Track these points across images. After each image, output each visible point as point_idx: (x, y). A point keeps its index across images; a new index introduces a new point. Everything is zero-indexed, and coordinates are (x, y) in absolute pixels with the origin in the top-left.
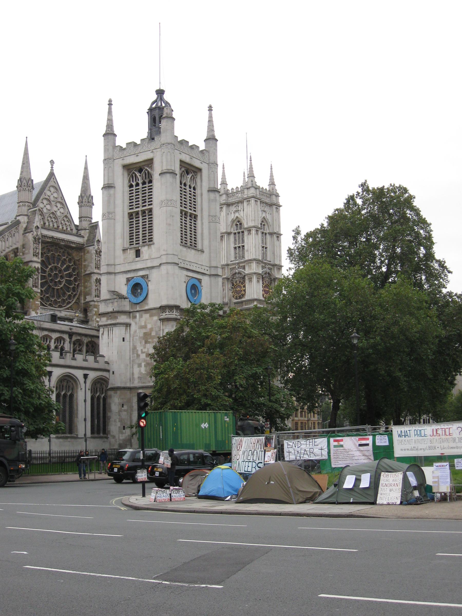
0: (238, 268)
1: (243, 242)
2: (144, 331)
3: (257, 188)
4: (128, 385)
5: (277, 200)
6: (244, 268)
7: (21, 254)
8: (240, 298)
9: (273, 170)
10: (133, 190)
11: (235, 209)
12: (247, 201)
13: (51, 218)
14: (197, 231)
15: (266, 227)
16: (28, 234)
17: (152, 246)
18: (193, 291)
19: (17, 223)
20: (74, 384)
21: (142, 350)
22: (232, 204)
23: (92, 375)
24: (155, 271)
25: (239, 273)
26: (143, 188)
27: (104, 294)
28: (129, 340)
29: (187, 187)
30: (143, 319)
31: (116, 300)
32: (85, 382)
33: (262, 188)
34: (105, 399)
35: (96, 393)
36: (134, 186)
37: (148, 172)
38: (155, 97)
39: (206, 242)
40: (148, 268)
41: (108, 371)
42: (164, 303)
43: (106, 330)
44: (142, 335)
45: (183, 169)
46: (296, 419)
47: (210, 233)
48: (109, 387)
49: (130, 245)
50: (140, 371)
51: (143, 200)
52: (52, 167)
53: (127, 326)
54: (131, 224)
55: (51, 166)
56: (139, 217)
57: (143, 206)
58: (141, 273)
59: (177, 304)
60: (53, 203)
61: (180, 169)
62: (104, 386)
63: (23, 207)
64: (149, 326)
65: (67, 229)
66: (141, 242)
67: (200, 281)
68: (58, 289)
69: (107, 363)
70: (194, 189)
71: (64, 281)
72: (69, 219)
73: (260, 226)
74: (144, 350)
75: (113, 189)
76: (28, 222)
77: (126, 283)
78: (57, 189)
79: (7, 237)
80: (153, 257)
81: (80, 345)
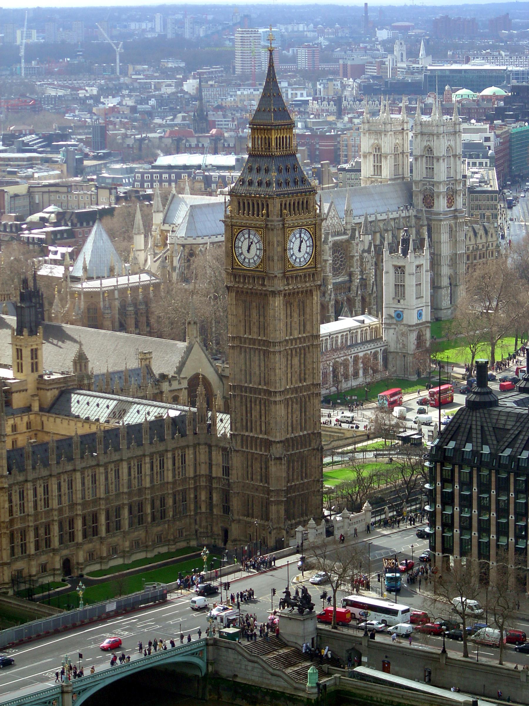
6: (433, 185)
8: (430, 208)
11: (427, 139)
23: (383, 348)
46: (475, 262)
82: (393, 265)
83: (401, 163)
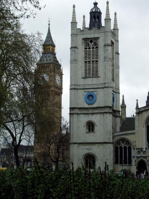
38: (93, 5)
54: (86, 66)
82: (83, 39)
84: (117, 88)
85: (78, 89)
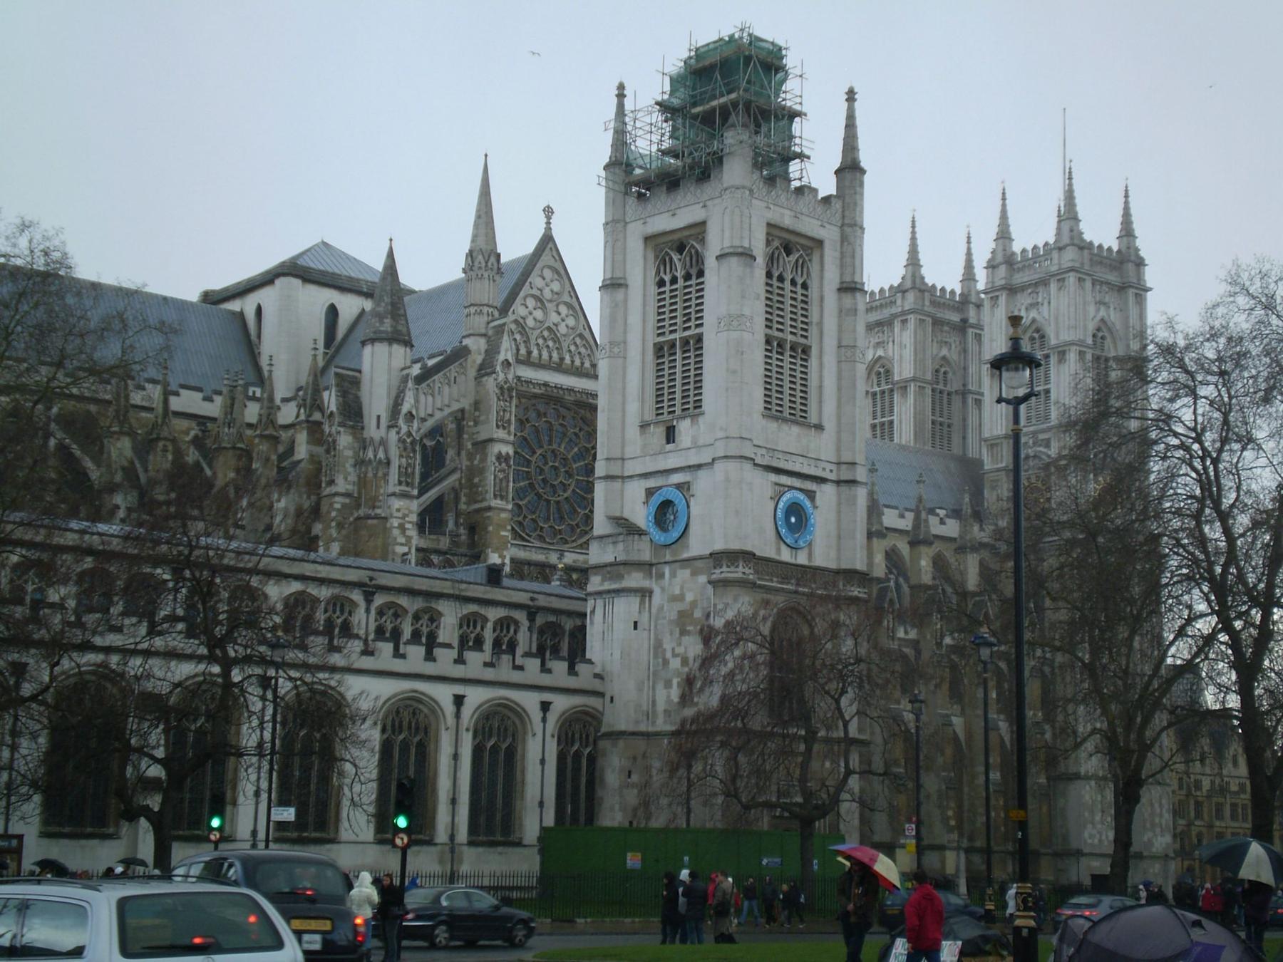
0: (1034, 443)
1: (891, 411)
2: (679, 606)
3: (1084, 247)
4: (642, 728)
5: (1140, 276)
7: (471, 423)
9: (1130, 199)
10: (664, 292)
11: (1029, 301)
12: (1059, 280)
13: (545, 339)
14: (809, 384)
15: (1108, 341)
16: (486, 378)
17: (701, 419)
18: (793, 520)
19: (460, 354)
20: (517, 722)
21: (673, 649)
22: (1022, 288)
23: (561, 704)
24: (702, 474)
25: (1035, 457)
26: (686, 287)
27: (600, 525)
28: (647, 627)
29: (787, 285)
30: (678, 580)
31: (621, 538)
32: (544, 720)
33: (1100, 247)
34: (592, 759)
35: (572, 745)
36: (668, 284)
37: (697, 252)
39: (829, 407)
40: (689, 467)
41: (601, 694)
42: (719, 546)
43: (600, 603)
44: (674, 616)
45: (776, 243)
47: (839, 389)
48: (603, 730)
49: (657, 415)
50: (669, 697)
51: (685, 315)
52: (548, 223)
53: (643, 596)
55: (545, 220)
56: (675, 354)
57: (685, 329)
58: (677, 478)
59: (748, 548)
60: (548, 305)
61: (768, 243)
62: (592, 729)
63: (477, 317)
64: (689, 597)
65: (582, 364)
66: (678, 409)
67: (811, 495)
68: (558, 503)
69: (597, 676)
70: (805, 286)
71: (572, 483)
72: (587, 341)
73: (1090, 341)
74: (678, 650)
75: (622, 290)
76: (486, 351)
77: (643, 499)
78: (561, 272)
79: (438, 385)
80: (701, 442)
81: (555, 635)
82: (648, 239)
83: (956, 420)
84: (844, 459)
85: (623, 478)
